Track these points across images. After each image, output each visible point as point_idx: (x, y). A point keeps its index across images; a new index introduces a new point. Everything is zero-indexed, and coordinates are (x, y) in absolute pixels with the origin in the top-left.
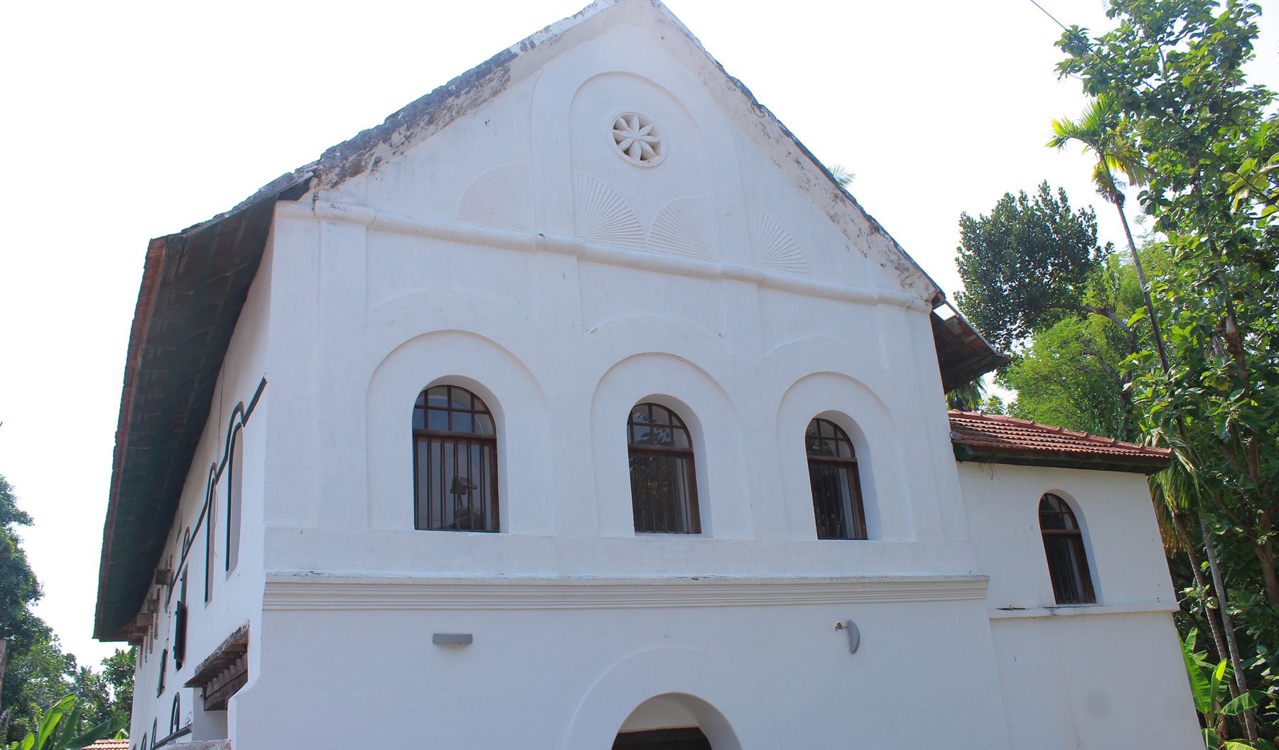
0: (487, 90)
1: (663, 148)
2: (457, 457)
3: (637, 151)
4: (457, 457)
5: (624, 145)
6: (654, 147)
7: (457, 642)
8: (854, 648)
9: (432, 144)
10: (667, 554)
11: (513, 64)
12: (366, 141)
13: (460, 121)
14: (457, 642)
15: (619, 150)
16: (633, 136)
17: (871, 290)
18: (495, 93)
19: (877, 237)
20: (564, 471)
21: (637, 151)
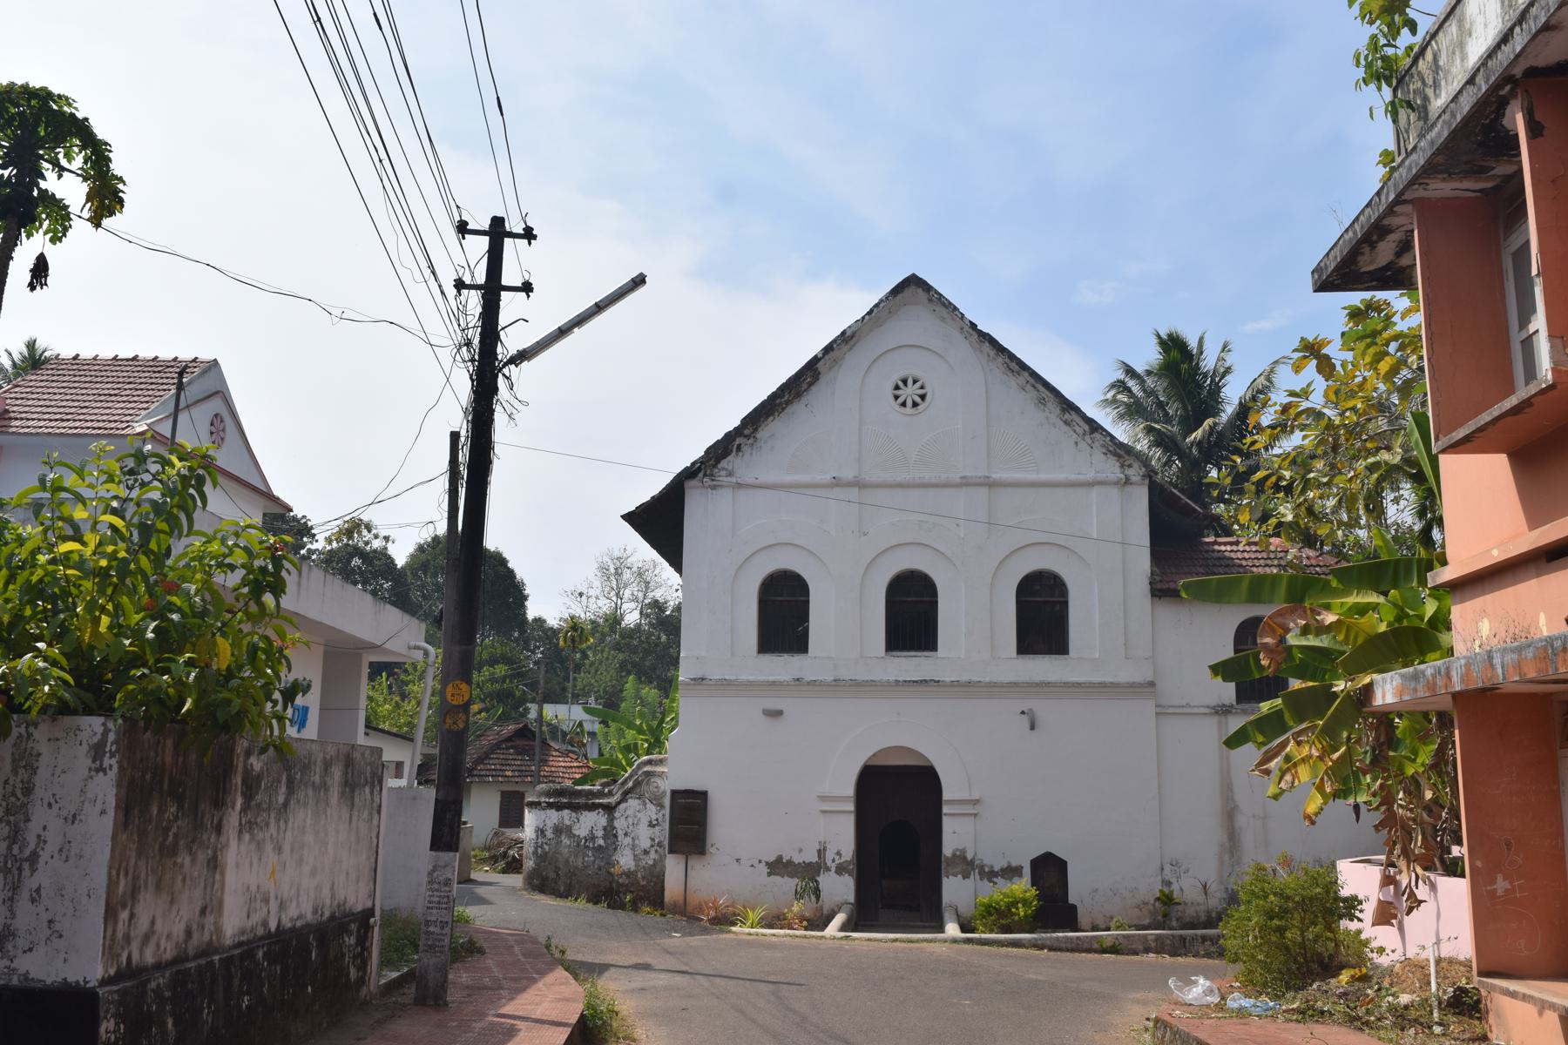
0: (805, 386)
1: (928, 398)
2: (783, 614)
3: (909, 403)
4: (783, 614)
5: (900, 400)
6: (923, 397)
7: (776, 714)
8: (1032, 728)
9: (771, 427)
10: (911, 665)
11: (820, 365)
12: (729, 437)
13: (790, 409)
14: (776, 714)
15: (896, 405)
16: (910, 392)
17: (1090, 475)
18: (811, 384)
19: (1097, 435)
20: (846, 620)
21: (909, 403)
